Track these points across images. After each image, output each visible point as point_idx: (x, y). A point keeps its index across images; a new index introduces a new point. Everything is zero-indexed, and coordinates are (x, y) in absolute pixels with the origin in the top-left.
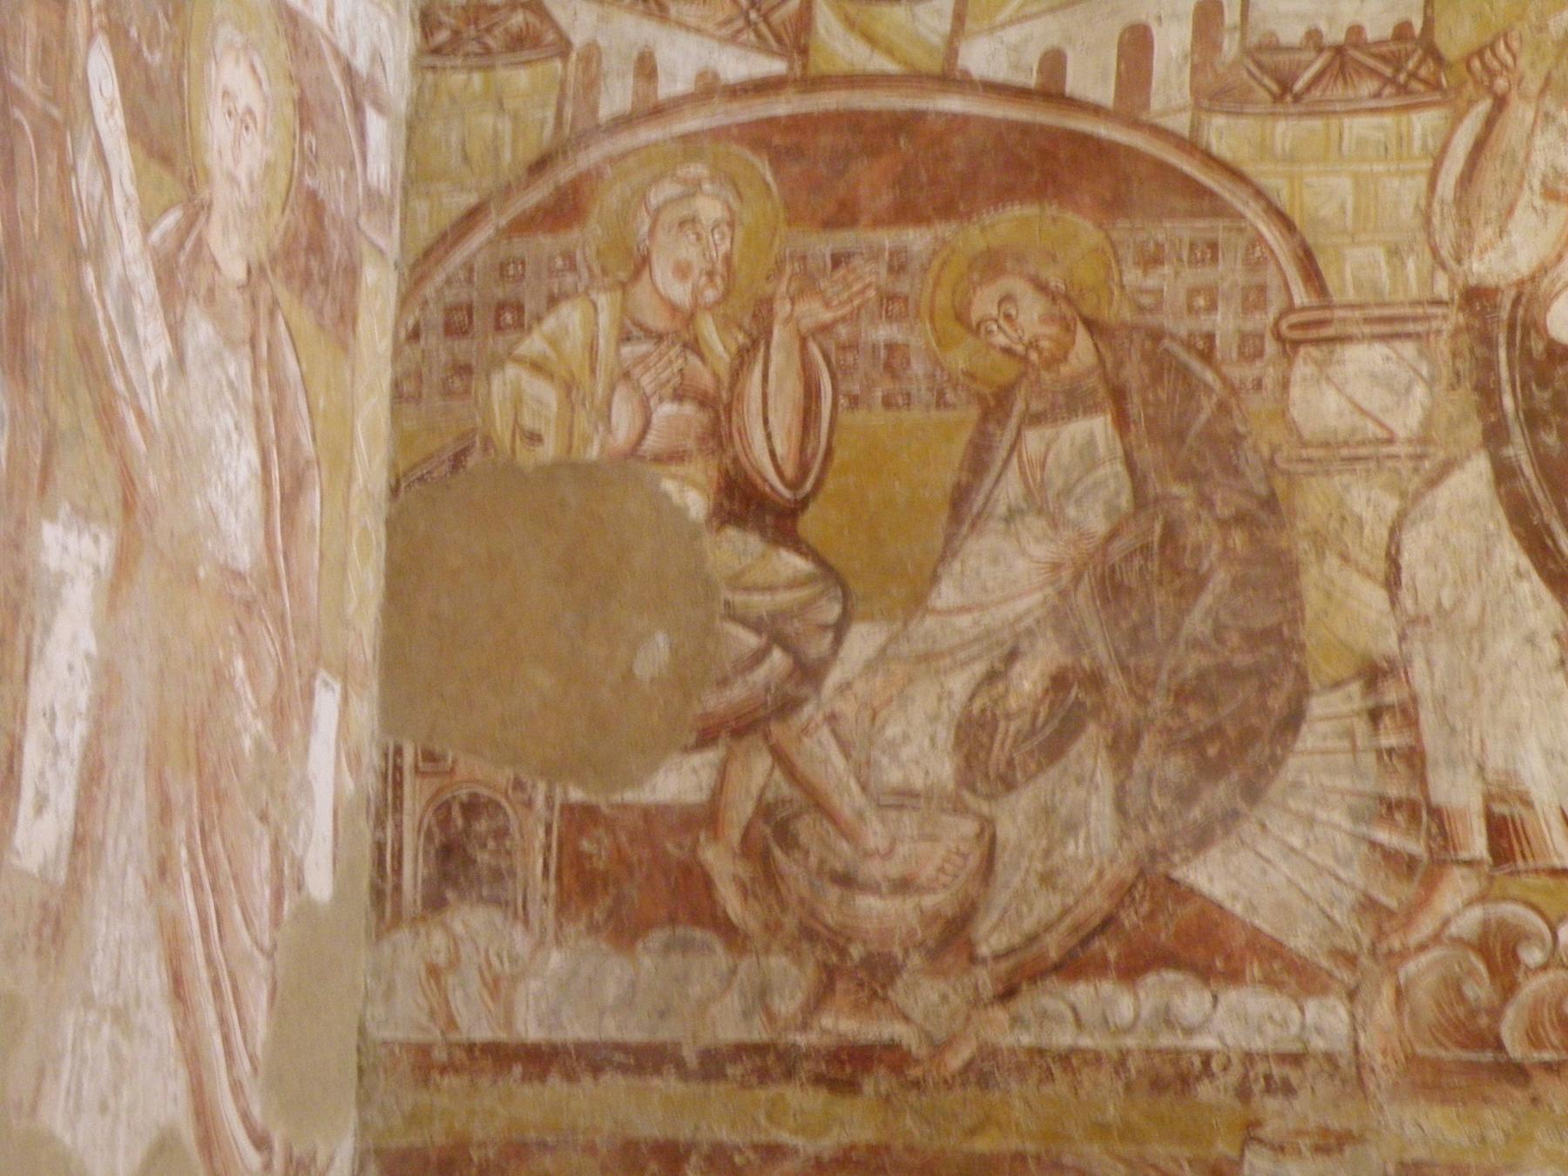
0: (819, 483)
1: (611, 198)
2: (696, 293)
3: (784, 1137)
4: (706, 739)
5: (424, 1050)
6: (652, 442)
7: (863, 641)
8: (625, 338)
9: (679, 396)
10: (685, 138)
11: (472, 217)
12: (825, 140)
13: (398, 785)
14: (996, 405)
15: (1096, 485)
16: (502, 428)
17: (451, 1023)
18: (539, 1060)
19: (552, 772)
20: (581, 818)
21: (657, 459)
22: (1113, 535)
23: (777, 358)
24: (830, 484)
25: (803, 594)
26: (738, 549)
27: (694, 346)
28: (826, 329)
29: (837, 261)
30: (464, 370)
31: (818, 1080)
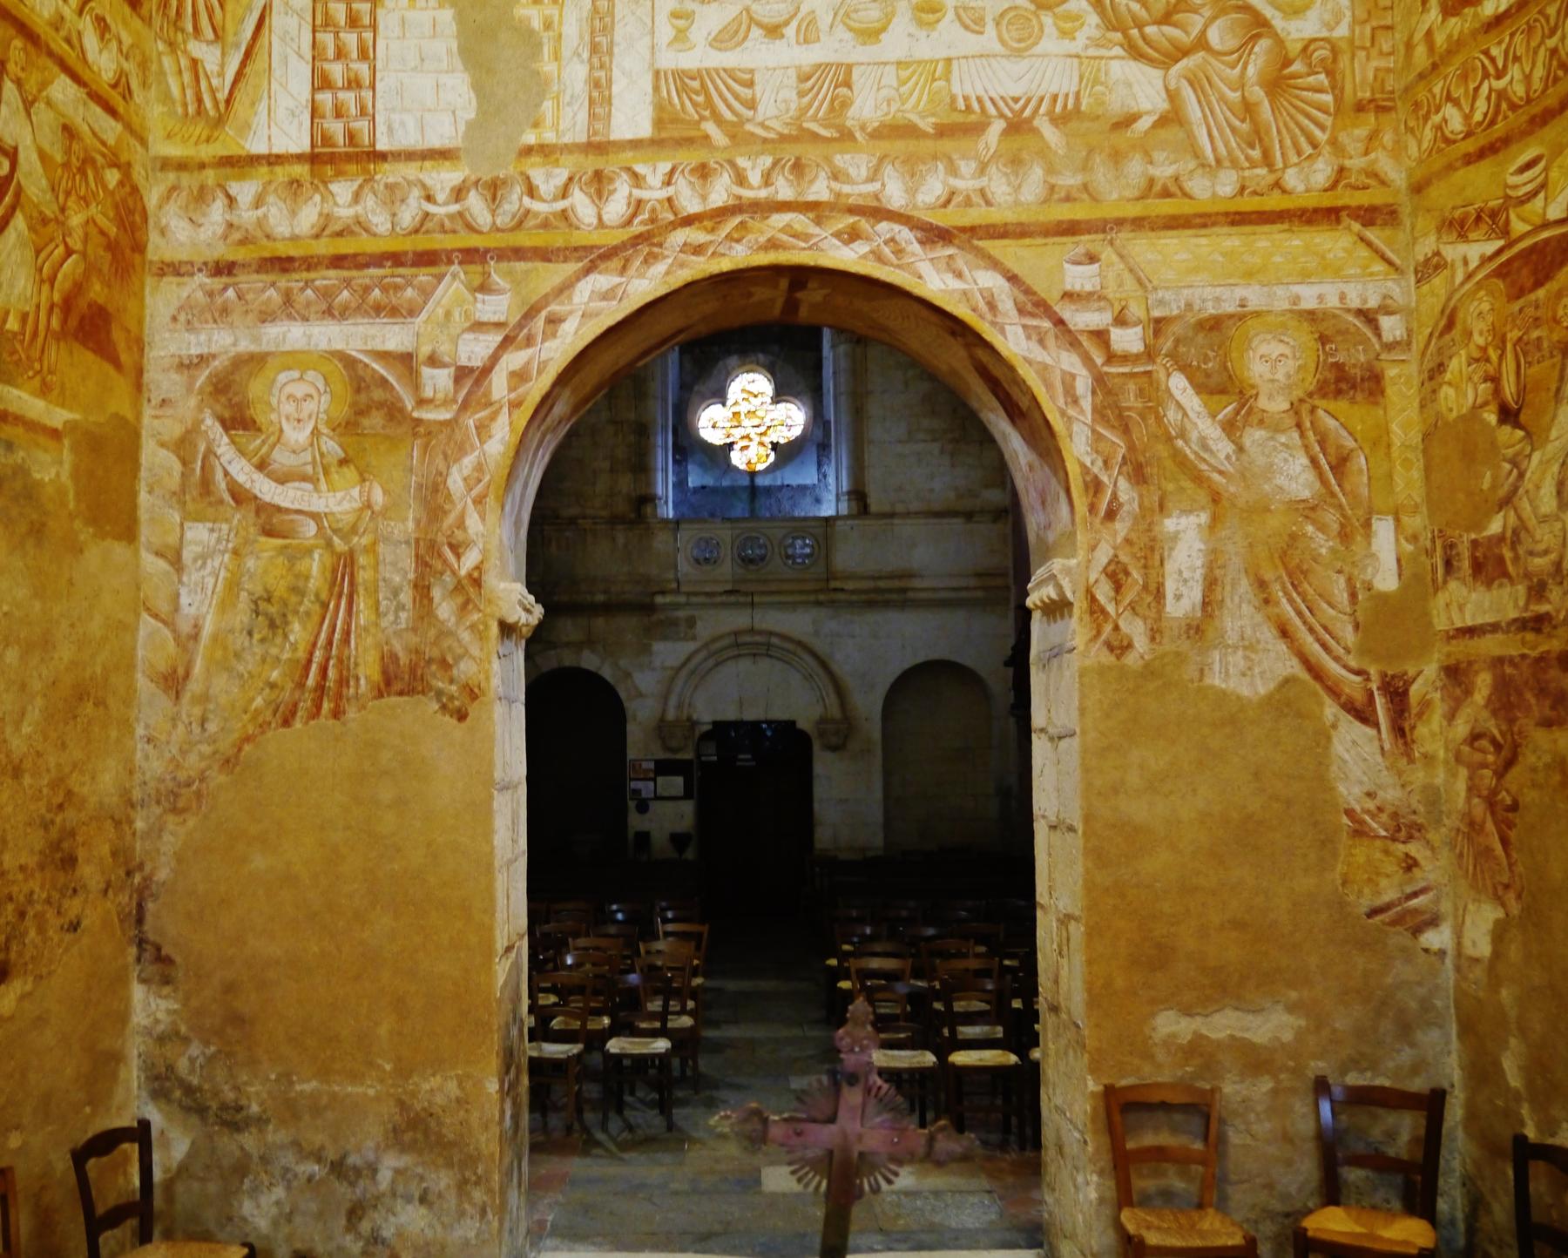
1: (1461, 315)
3: (1526, 651)
4: (1500, 509)
5: (1447, 632)
6: (1479, 401)
7: (1536, 457)
9: (1485, 381)
11: (1431, 335)
12: (1516, 264)
16: (1444, 409)
18: (1471, 631)
19: (1468, 530)
20: (1475, 543)
21: (1481, 407)
26: (1507, 434)
27: (1488, 360)
28: (1520, 339)
29: (1521, 310)
30: (1434, 391)
31: (1533, 629)
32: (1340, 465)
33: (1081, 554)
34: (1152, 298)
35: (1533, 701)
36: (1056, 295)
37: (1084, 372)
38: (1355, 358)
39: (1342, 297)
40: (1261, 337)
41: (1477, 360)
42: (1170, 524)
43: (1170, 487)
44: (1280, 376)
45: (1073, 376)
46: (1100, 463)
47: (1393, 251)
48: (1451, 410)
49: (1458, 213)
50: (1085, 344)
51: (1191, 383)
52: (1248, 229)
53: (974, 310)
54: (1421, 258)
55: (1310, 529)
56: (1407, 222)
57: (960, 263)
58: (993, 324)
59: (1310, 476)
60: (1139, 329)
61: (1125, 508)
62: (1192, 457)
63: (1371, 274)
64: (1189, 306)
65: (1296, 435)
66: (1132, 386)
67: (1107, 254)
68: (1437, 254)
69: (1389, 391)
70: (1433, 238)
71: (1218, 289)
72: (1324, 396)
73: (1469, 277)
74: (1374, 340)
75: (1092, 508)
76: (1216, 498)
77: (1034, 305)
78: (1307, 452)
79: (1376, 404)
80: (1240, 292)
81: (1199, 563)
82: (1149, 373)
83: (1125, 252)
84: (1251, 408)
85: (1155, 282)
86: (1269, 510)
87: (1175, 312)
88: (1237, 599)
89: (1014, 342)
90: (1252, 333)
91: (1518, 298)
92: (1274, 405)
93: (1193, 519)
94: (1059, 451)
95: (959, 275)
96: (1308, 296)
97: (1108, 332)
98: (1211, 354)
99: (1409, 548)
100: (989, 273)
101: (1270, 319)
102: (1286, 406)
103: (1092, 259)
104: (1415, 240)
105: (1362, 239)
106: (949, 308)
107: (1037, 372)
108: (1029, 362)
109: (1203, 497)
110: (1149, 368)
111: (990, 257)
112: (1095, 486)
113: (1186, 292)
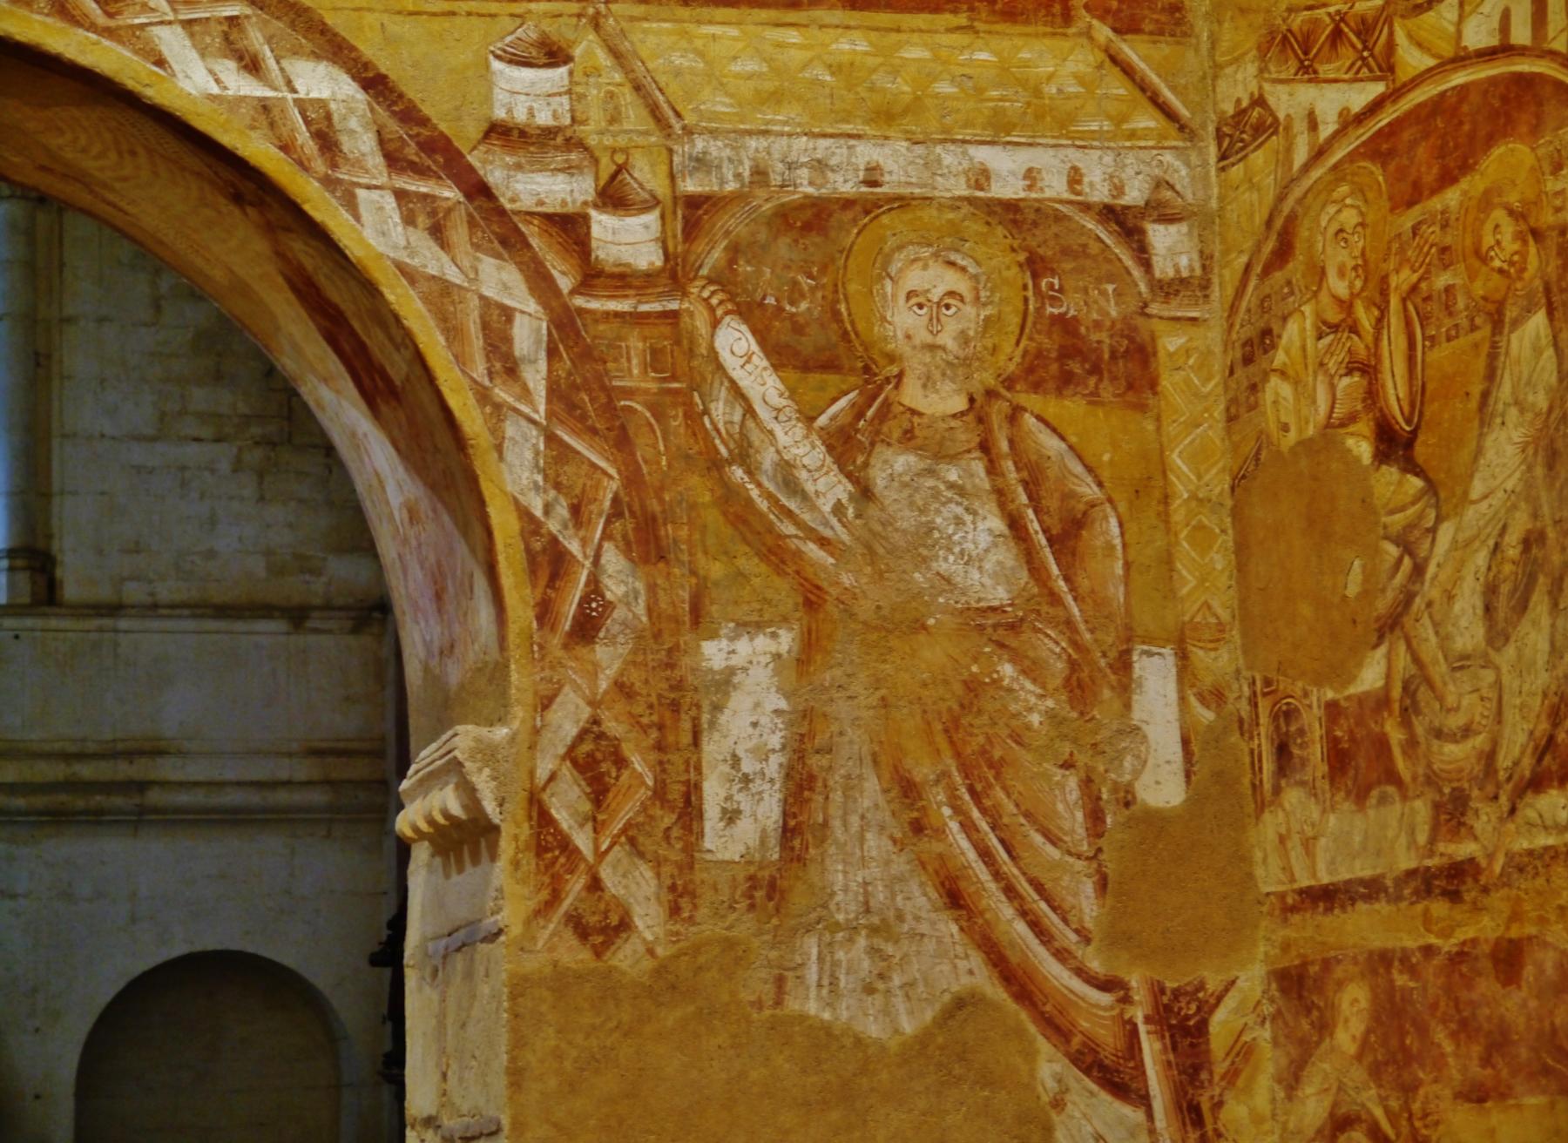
0: (1421, 414)
1: (1303, 233)
2: (1351, 286)
3: (1433, 940)
4: (1381, 638)
6: (1339, 412)
7: (1446, 533)
8: (1320, 338)
9: (1349, 372)
10: (1335, 167)
11: (1248, 268)
12: (1407, 135)
13: (1256, 705)
14: (1497, 323)
15: (1543, 369)
16: (1273, 427)
17: (1293, 880)
18: (1326, 897)
19: (1319, 681)
20: (1333, 709)
22: (1550, 410)
23: (1393, 320)
24: (1427, 414)
25: (1418, 506)
27: (1354, 329)
28: (1414, 288)
29: (1415, 230)
30: (1253, 388)
32: (1069, 534)
33: (520, 715)
34: (682, 151)
35: (1448, 1047)
36: (474, 130)
37: (532, 306)
38: (1099, 307)
39: (1075, 178)
40: (911, 251)
41: (1335, 328)
42: (714, 653)
43: (716, 570)
44: (947, 339)
45: (508, 314)
46: (562, 511)
47: (1173, 89)
48: (1285, 428)
49: (1298, 21)
50: (535, 242)
51: (762, 343)
52: (884, 18)
53: (285, 148)
54: (1229, 109)
55: (1007, 670)
56: (1202, 29)
57: (255, 39)
58: (329, 183)
59: (1006, 555)
60: (652, 218)
61: (619, 613)
62: (763, 505)
63: (1132, 135)
64: (760, 174)
65: (979, 467)
66: (635, 343)
67: (587, 47)
68: (1259, 101)
69: (1166, 383)
70: (1251, 69)
71: (823, 143)
72: (1036, 387)
73: (1319, 154)
74: (1137, 273)
75: (545, 612)
76: (812, 598)
77: (419, 146)
78: (1002, 506)
79: (1142, 408)
80: (866, 153)
81: (775, 741)
82: (674, 315)
83: (625, 46)
84: (887, 404)
85: (690, 119)
86: (924, 627)
87: (731, 186)
88: (855, 820)
89: (375, 227)
90: (891, 242)
91: (1410, 204)
92: (941, 401)
93: (762, 642)
94: (473, 480)
95: (252, 66)
96: (1005, 171)
97: (586, 218)
98: (806, 283)
99: (1207, 715)
100: (323, 68)
101: (929, 214)
102: (960, 404)
103: (554, 55)
104: (1218, 68)
105: (1114, 60)
106: (226, 139)
107: (426, 300)
108: (409, 275)
109: (784, 593)
110: (673, 305)
111: (324, 30)
112: (550, 563)
113: (753, 143)
